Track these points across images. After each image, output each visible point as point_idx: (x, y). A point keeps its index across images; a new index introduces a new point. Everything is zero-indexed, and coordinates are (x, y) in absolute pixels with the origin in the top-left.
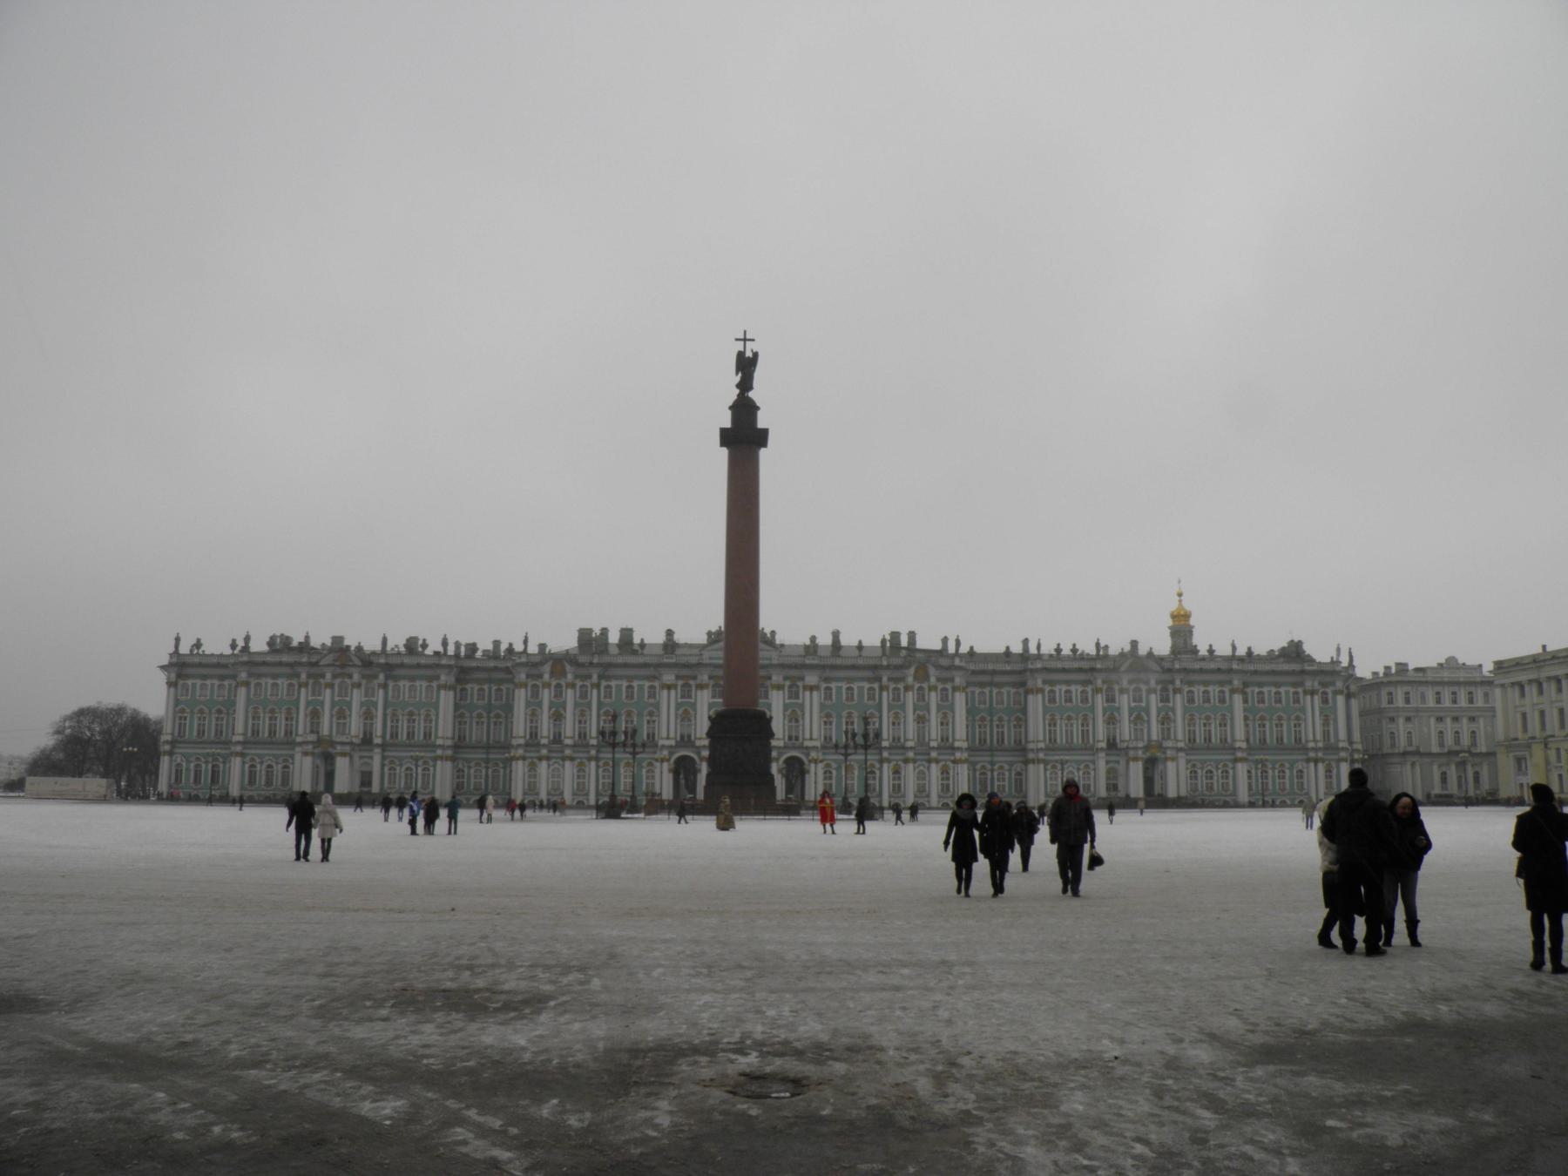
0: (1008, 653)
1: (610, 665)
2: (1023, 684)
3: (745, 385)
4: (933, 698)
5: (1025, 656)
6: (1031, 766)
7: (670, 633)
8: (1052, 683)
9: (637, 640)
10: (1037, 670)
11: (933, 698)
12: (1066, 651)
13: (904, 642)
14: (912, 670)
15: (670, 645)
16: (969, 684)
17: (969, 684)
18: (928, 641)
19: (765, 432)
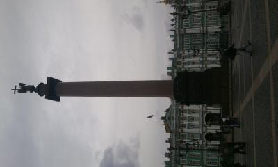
0: (173, 40)
1: (176, 160)
2: (183, 35)
3: (31, 89)
4: (187, 60)
5: (175, 36)
6: (209, 31)
7: (166, 141)
8: (182, 26)
9: (168, 152)
10: (179, 31)
11: (187, 60)
12: (174, 22)
13: (170, 71)
14: (178, 66)
15: (169, 141)
16: (183, 49)
17: (183, 49)
18: (170, 64)
19: (50, 79)
